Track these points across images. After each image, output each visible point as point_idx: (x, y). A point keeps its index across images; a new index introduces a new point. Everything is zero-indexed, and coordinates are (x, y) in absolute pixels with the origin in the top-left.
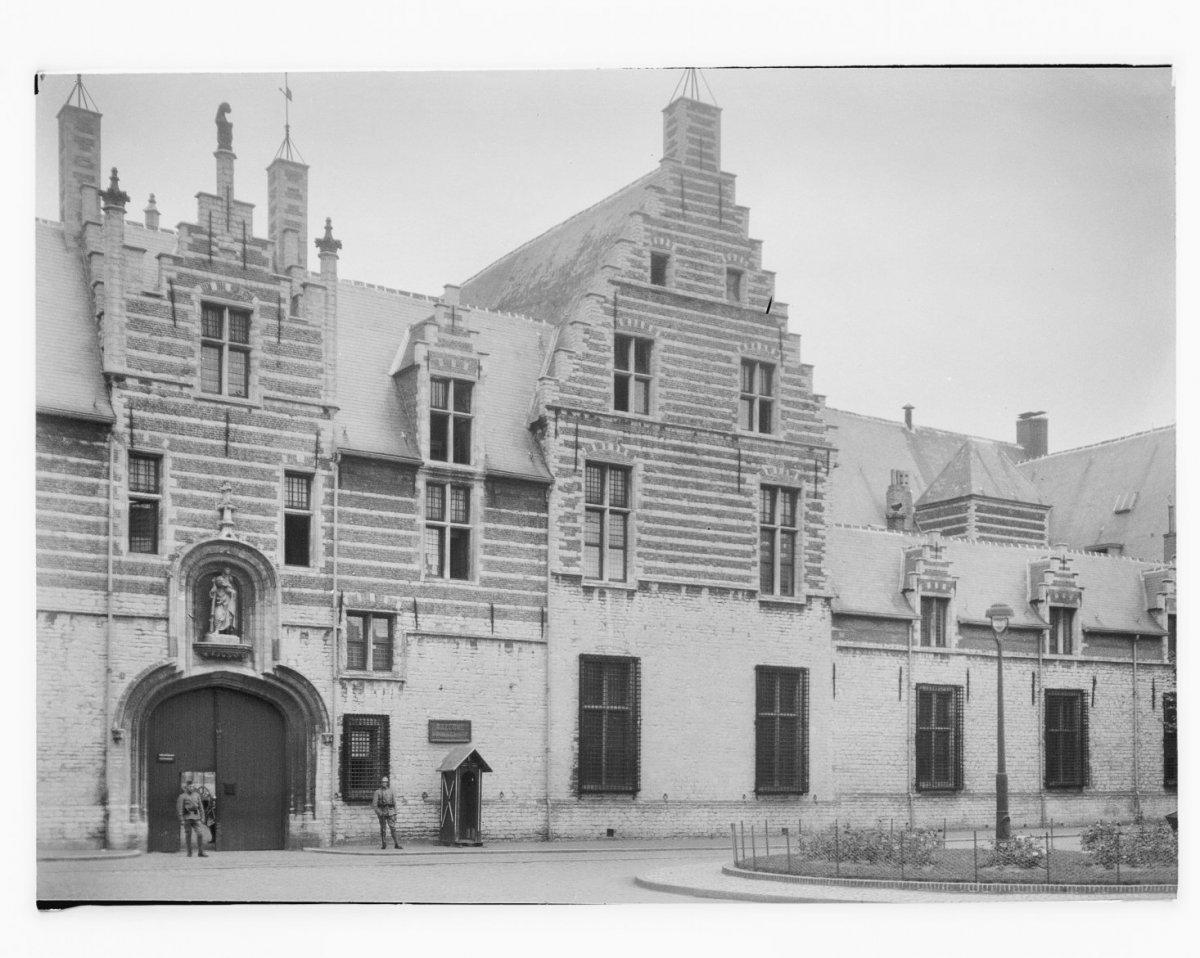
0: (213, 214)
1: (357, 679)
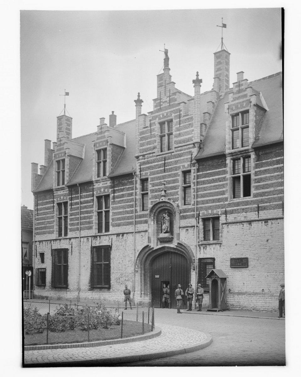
0: (161, 92)
1: (204, 244)
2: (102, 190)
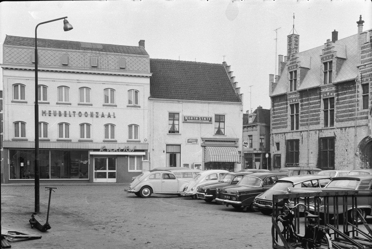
2: (328, 94)
